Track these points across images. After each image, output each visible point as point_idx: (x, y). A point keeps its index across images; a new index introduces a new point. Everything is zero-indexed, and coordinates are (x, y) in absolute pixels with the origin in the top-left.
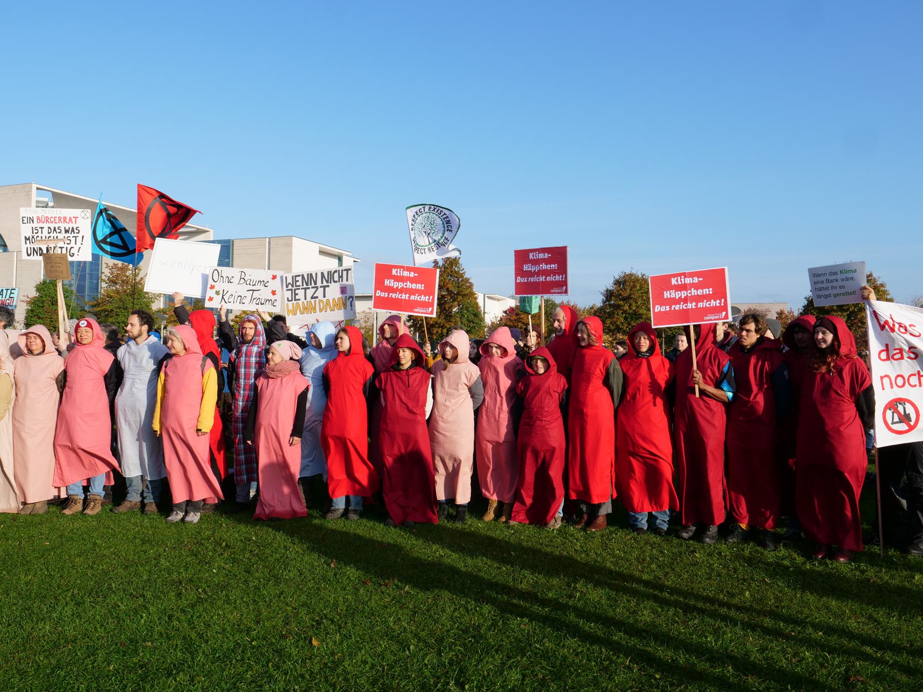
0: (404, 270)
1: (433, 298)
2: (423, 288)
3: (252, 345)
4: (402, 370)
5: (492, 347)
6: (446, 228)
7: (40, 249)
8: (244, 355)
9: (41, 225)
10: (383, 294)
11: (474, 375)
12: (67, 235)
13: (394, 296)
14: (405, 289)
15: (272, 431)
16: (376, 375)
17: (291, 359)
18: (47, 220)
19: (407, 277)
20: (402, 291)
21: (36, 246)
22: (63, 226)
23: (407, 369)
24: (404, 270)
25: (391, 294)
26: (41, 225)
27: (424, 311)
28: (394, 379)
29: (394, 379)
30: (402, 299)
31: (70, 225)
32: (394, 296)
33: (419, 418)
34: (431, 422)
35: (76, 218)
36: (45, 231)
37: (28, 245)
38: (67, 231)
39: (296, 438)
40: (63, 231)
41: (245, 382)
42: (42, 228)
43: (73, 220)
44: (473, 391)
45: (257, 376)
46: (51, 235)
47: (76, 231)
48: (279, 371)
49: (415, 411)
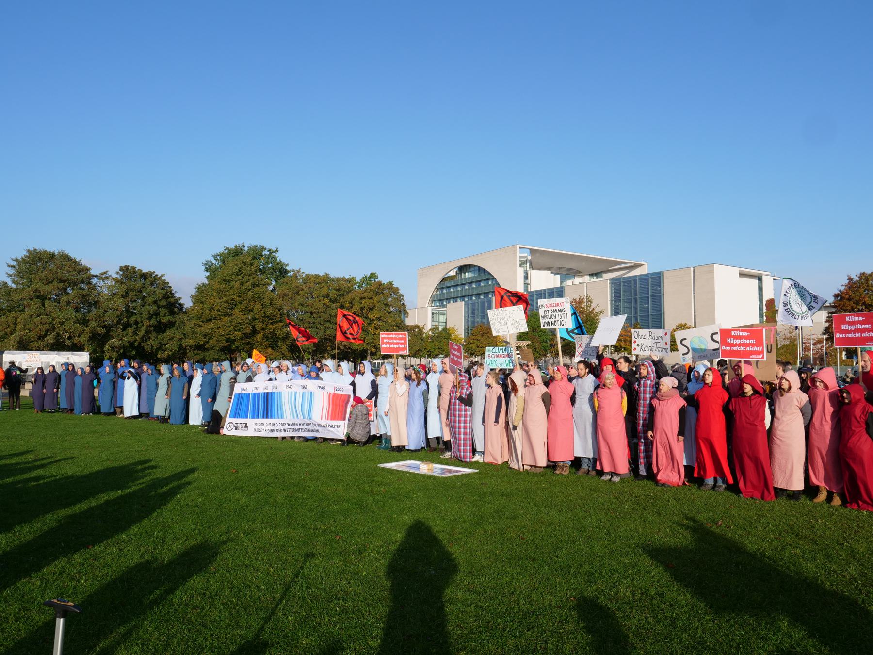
0: (739, 332)
1: (763, 348)
2: (754, 342)
3: (647, 380)
4: (746, 396)
5: (817, 381)
6: (813, 300)
7: (549, 322)
8: (642, 386)
9: (548, 309)
10: (727, 348)
11: (803, 400)
12: (560, 313)
13: (734, 348)
14: (742, 343)
15: (664, 433)
16: (730, 400)
17: (673, 387)
18: (550, 305)
19: (742, 336)
20: (740, 345)
21: (547, 320)
22: (558, 308)
23: (750, 396)
24: (739, 332)
25: (732, 348)
26: (548, 309)
27: (757, 357)
28: (741, 402)
29: (741, 402)
30: (740, 351)
31: (560, 308)
32: (734, 348)
33: (759, 428)
34: (770, 433)
35: (563, 303)
36: (550, 311)
37: (543, 321)
38: (559, 311)
39: (680, 437)
40: (558, 311)
41: (643, 402)
42: (548, 310)
43: (562, 304)
44: (803, 411)
45: (651, 399)
46: (553, 314)
47: (564, 311)
48: (667, 396)
49: (756, 424)
